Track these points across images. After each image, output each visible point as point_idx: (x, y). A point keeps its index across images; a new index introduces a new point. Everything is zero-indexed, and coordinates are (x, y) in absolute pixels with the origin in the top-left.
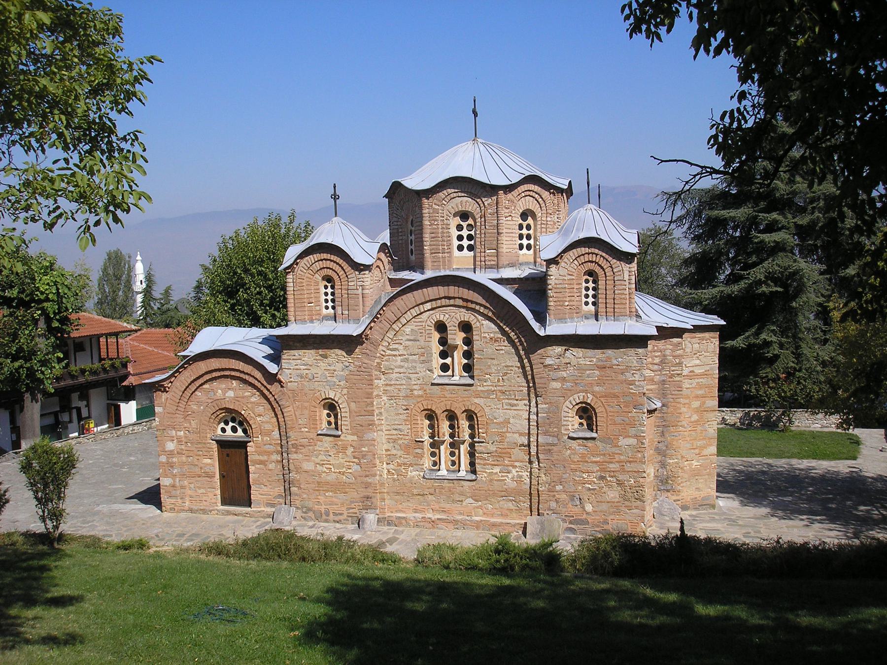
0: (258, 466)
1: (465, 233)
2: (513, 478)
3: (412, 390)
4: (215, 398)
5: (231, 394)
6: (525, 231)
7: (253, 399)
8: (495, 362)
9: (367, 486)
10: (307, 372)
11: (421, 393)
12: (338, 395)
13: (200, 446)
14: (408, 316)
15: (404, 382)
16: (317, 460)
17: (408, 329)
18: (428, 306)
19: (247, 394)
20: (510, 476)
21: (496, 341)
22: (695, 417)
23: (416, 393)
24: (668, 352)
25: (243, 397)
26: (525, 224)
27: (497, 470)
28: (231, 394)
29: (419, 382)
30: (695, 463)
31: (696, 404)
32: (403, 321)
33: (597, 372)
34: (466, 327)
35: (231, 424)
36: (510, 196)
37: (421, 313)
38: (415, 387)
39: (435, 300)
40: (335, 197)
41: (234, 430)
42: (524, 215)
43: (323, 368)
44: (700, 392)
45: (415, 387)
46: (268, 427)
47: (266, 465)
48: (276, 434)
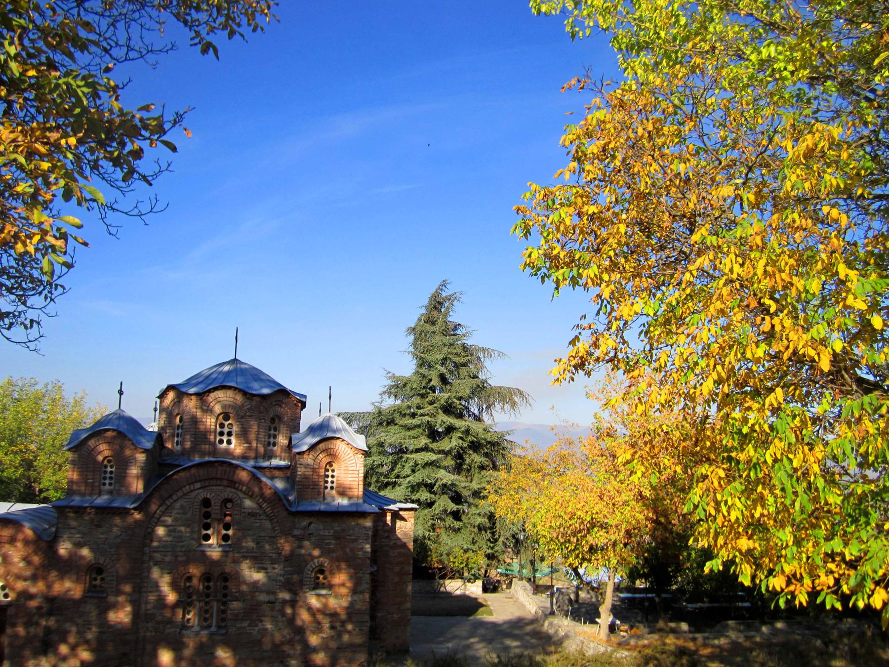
1: (226, 430)
2: (258, 631)
3: (177, 556)
6: (272, 432)
11: (184, 558)
12: (108, 560)
14: (179, 494)
15: (170, 549)
17: (178, 505)
18: (198, 485)
20: (257, 629)
21: (253, 516)
22: (396, 579)
23: (180, 559)
24: (380, 528)
26: (273, 426)
27: (245, 624)
29: (183, 549)
30: (396, 616)
31: (397, 569)
32: (175, 497)
33: (333, 542)
36: (265, 404)
37: (191, 491)
38: (180, 554)
39: (205, 480)
40: (121, 392)
42: (273, 420)
44: (401, 559)
45: (180, 554)
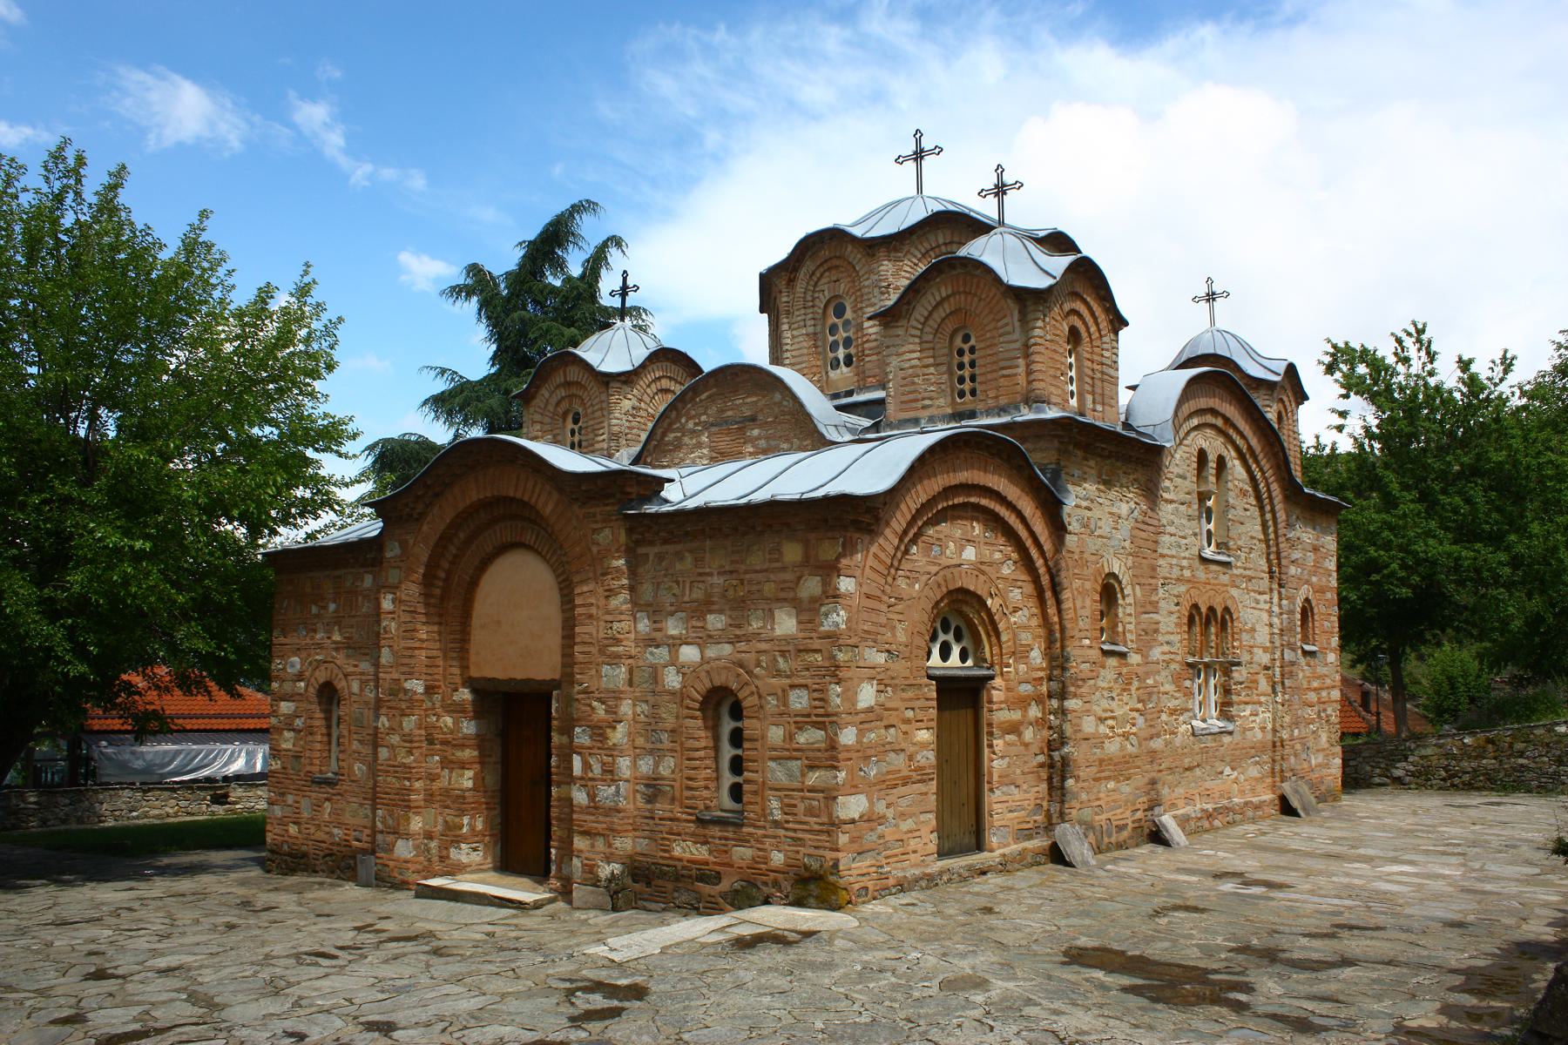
0: (1008, 737)
4: (945, 562)
5: (970, 553)
7: (1006, 570)
8: (1242, 529)
9: (1153, 753)
10: (1089, 514)
13: (910, 694)
16: (1098, 710)
19: (998, 555)
25: (991, 564)
28: (970, 553)
29: (1186, 554)
34: (1221, 461)
35: (942, 637)
41: (945, 654)
43: (1107, 509)
46: (1026, 637)
47: (1020, 735)
48: (1036, 656)
